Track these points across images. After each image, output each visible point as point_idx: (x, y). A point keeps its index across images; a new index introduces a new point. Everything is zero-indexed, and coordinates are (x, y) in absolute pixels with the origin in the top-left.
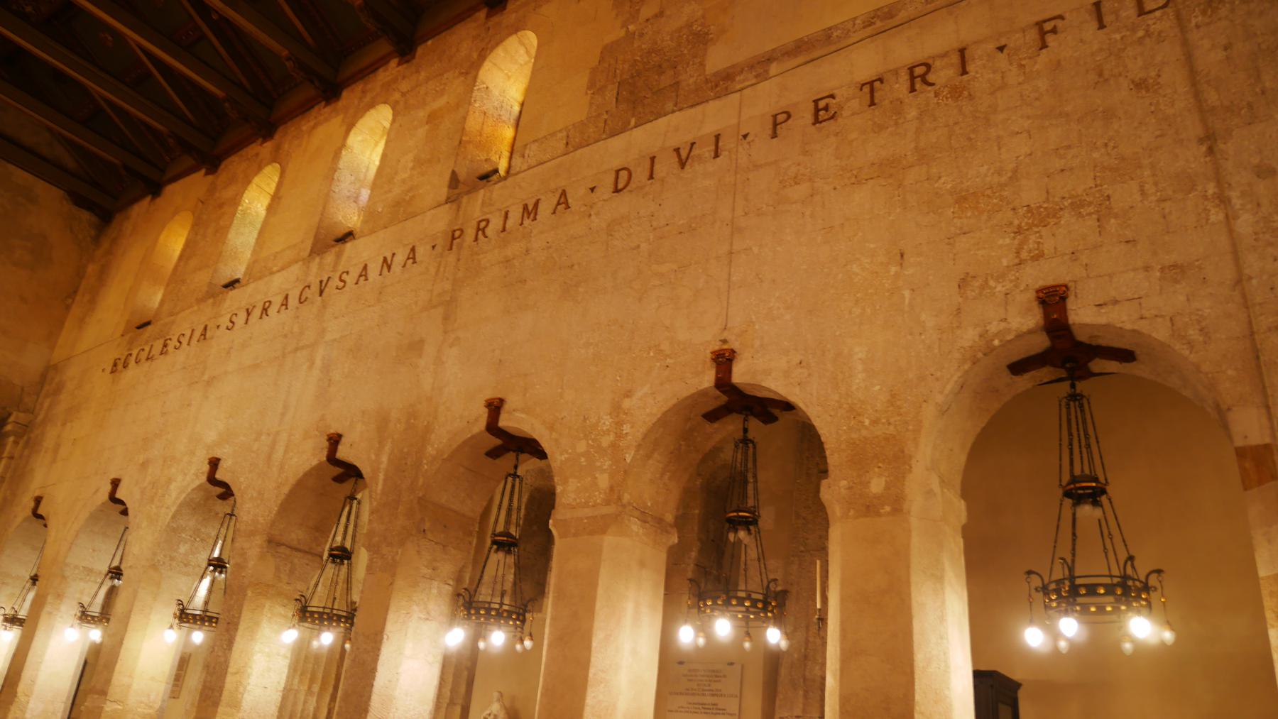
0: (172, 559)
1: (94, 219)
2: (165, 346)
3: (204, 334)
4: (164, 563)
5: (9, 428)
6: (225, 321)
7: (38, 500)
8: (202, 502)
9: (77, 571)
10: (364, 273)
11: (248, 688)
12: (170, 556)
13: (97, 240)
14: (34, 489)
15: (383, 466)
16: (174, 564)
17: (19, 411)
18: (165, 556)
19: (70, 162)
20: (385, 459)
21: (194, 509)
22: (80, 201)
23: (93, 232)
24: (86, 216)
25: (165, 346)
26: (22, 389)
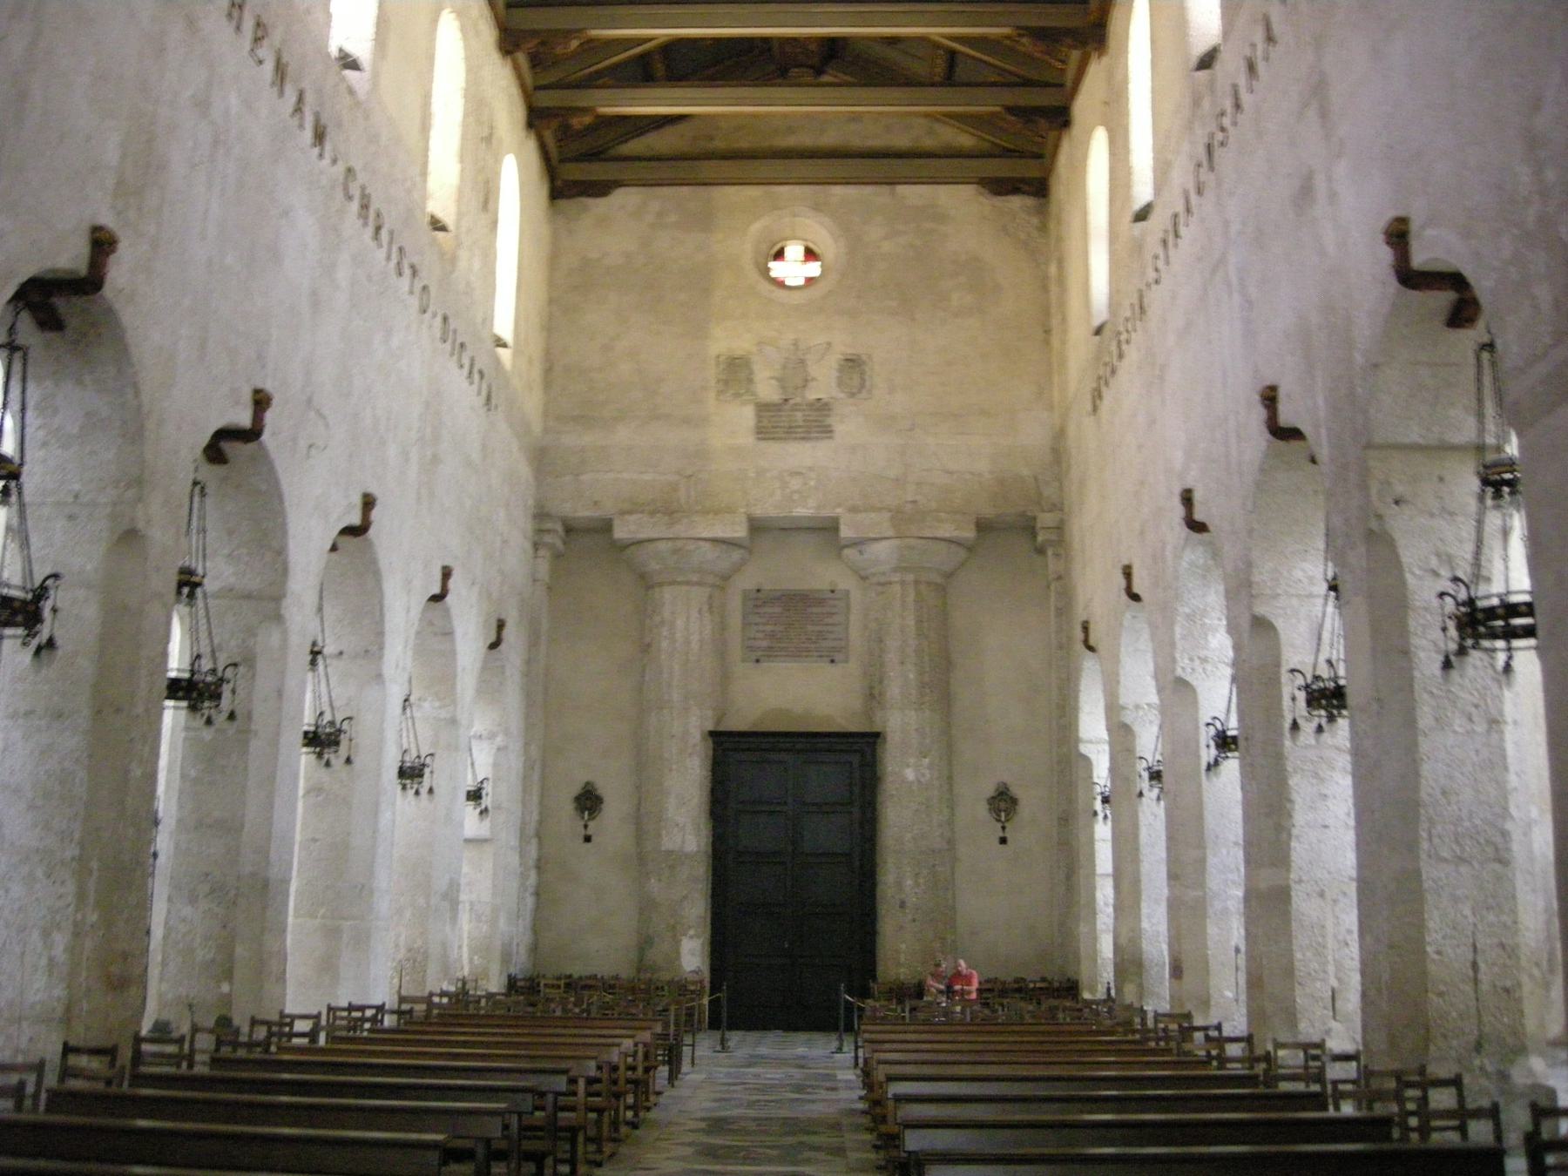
0: (1204, 660)
1: (1029, 201)
2: (1119, 342)
3: (1141, 308)
4: (1193, 669)
5: (1040, 539)
6: (1152, 275)
7: (1086, 628)
8: (1210, 562)
9: (1141, 713)
10: (1238, 106)
11: (1295, 832)
12: (1199, 658)
13: (1043, 228)
14: (1081, 615)
15: (1322, 414)
16: (1209, 667)
17: (1043, 511)
18: (1191, 660)
19: (965, 140)
20: (1321, 401)
21: (1204, 577)
22: (1001, 187)
23: (1035, 221)
24: (1016, 202)
25: (1119, 342)
26: (1036, 479)
